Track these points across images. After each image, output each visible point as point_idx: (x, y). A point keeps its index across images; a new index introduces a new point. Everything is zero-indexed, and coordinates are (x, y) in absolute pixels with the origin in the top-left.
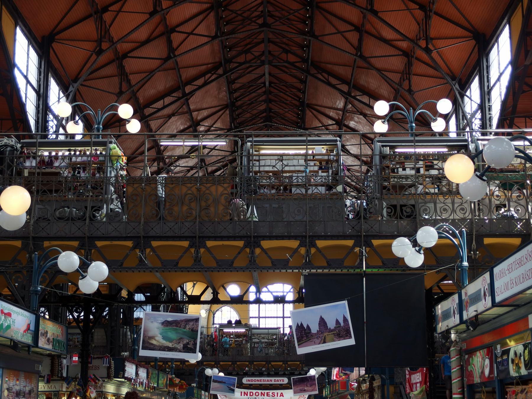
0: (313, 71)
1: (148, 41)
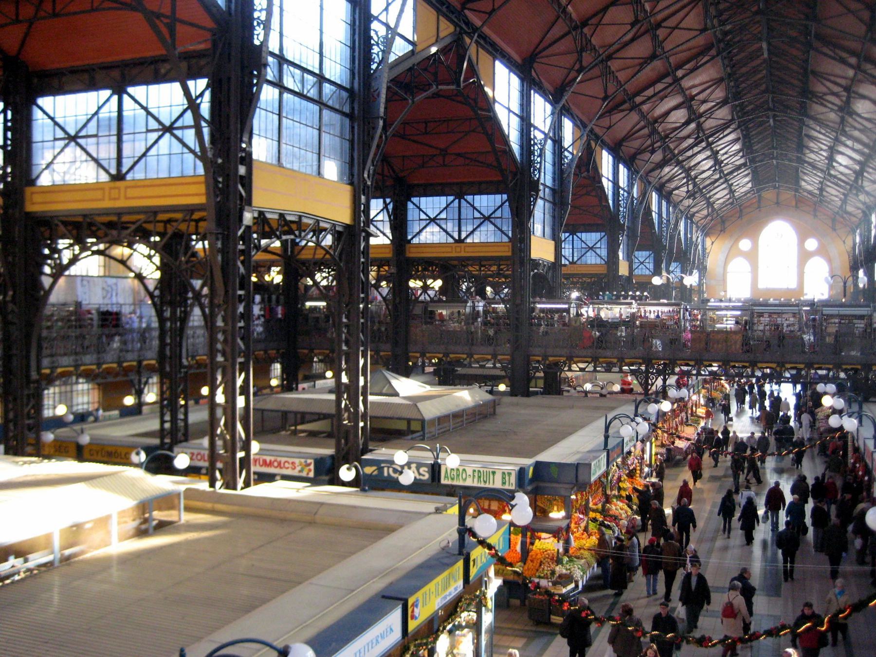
0: (816, 44)
1: (633, 40)
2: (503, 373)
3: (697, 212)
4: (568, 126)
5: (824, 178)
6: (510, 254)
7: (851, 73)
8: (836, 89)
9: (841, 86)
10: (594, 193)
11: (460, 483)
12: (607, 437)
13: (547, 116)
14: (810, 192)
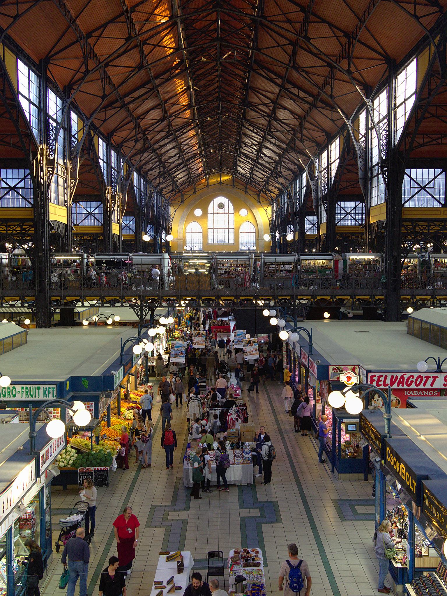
0: (256, 67)
2: (30, 311)
3: (165, 188)
4: (74, 116)
5: (254, 165)
6: (32, 217)
7: (277, 90)
8: (267, 101)
9: (269, 98)
10: (93, 171)
11: (12, 398)
12: (121, 355)
13: (59, 108)
14: (243, 175)
